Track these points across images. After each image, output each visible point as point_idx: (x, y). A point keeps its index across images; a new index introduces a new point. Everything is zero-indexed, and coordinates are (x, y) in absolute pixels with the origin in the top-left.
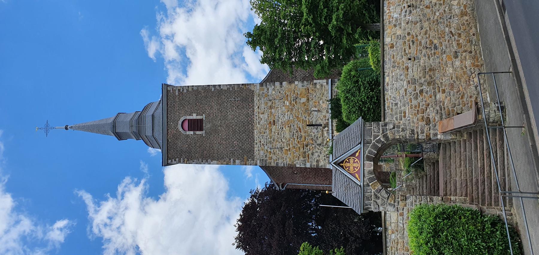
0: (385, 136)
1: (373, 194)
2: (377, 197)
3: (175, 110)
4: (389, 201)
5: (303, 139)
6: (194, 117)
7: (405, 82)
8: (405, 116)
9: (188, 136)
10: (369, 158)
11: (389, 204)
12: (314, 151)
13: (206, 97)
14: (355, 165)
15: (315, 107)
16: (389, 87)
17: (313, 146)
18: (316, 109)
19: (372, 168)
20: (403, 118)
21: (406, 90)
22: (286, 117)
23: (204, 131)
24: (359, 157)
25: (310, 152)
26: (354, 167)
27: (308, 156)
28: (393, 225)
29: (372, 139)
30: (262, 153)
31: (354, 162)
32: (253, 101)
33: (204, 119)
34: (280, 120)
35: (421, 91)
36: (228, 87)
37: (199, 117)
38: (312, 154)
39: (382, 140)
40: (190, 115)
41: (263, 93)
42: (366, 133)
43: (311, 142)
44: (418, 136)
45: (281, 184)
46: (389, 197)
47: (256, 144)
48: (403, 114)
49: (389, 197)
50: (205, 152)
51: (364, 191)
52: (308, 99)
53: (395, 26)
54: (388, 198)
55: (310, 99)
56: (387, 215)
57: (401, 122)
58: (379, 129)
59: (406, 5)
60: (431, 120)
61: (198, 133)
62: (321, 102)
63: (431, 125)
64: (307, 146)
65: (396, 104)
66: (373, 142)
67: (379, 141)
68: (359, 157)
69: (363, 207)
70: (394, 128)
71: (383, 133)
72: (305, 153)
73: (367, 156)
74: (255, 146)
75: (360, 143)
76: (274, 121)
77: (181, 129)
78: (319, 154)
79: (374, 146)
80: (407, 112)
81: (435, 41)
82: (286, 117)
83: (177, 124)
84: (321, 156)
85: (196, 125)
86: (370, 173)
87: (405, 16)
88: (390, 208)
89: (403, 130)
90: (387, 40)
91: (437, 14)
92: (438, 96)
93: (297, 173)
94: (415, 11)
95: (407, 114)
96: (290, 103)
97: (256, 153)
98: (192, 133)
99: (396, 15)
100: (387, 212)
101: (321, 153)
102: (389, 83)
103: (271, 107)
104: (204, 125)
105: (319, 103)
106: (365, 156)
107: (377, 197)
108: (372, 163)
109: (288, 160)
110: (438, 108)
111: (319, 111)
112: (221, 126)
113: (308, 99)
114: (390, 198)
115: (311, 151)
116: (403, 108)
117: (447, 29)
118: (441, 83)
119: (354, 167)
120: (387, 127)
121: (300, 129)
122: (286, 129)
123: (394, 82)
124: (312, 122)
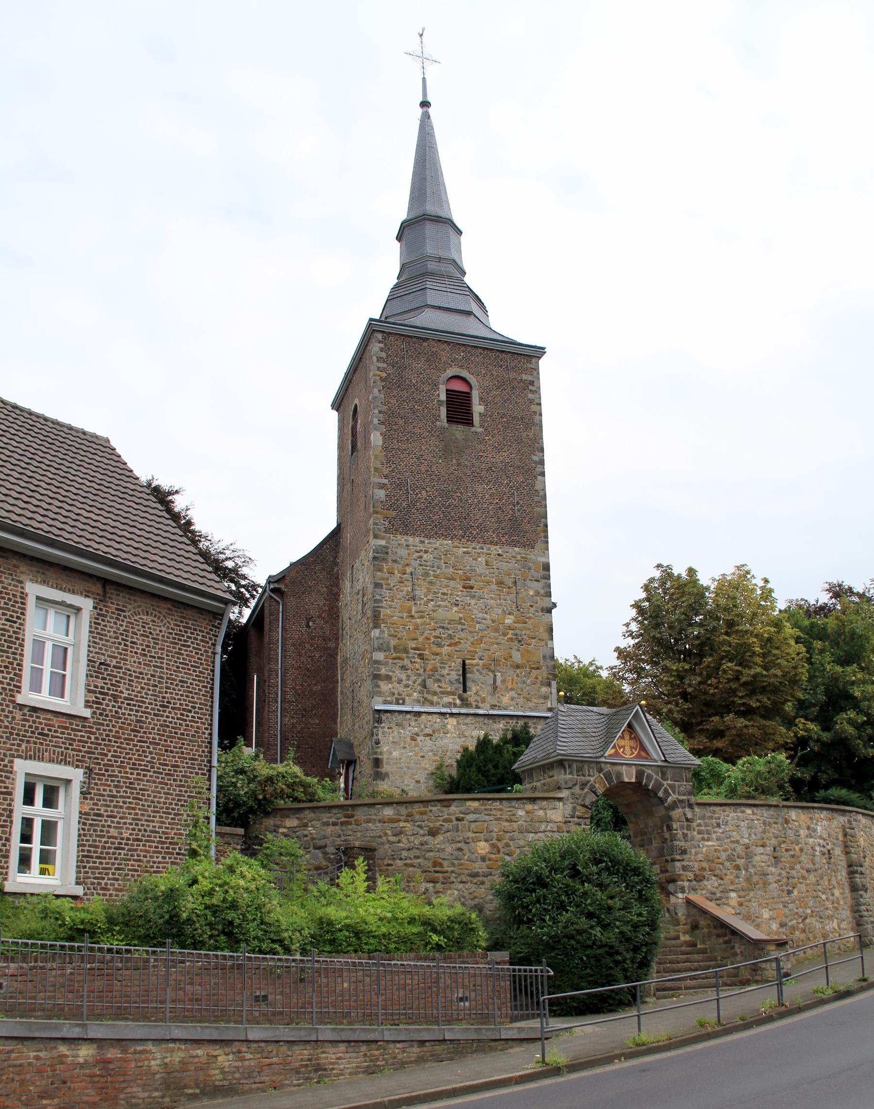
0: (674, 805)
1: (587, 778)
2: (583, 785)
3: (490, 367)
4: (579, 808)
5: (435, 649)
6: (477, 408)
7: (747, 841)
8: (703, 839)
9: (435, 386)
10: (640, 774)
11: (574, 808)
12: (409, 672)
13: (519, 441)
14: (627, 748)
15: (503, 681)
16: (739, 814)
17: (421, 671)
18: (498, 683)
19: (626, 780)
20: (700, 836)
21: (737, 842)
22: (480, 615)
23: (446, 425)
24: (639, 756)
25: (406, 662)
26: (624, 747)
27: (400, 658)
28: (541, 813)
29: (669, 782)
30: (403, 552)
31: (631, 748)
32: (513, 543)
33: (473, 429)
34: (473, 602)
35: (737, 868)
36: (541, 493)
37: (476, 419)
38: (403, 668)
39: (670, 799)
40: (481, 398)
41: (529, 569)
42: (677, 770)
43: (429, 667)
44: (679, 860)
45: (282, 587)
46: (586, 807)
47: (422, 542)
48: (706, 836)
49: (586, 807)
50: (402, 422)
51: (591, 762)
52: (518, 667)
53: (808, 828)
54: (584, 806)
55: (518, 671)
56: (557, 803)
57: (695, 833)
58: (684, 795)
59: (829, 847)
60: (701, 883)
61: (443, 411)
62: (512, 694)
63: (694, 882)
64: (421, 656)
65: (718, 825)
66: (665, 783)
67: (667, 794)
68: (639, 756)
69: (566, 760)
70: (687, 820)
71: (680, 801)
72: (406, 651)
73: (643, 772)
74: (417, 539)
75: (666, 761)
76: (472, 588)
77: (450, 373)
78: (404, 682)
79: (658, 785)
80: (710, 843)
81: (796, 892)
82: (480, 615)
83: (461, 367)
84: (400, 688)
85: (459, 408)
86: (619, 775)
87: (819, 845)
88: (569, 807)
89: (685, 836)
90: (793, 814)
91: (824, 897)
92: (733, 895)
93: (308, 626)
94: (824, 861)
95: (706, 843)
96: (510, 628)
97: (402, 539)
98: (443, 397)
99: (819, 829)
100: (561, 804)
101: (407, 686)
102: (745, 815)
103: (500, 583)
104: (461, 427)
105: (512, 689)
106: (643, 768)
107: (583, 785)
108: (633, 780)
109: (388, 611)
110: (718, 895)
111: (495, 688)
112: (459, 465)
113: (518, 667)
114: (583, 810)
115: (410, 665)
116: (714, 836)
117: (809, 911)
118: (750, 901)
119: (624, 747)
120: (687, 809)
121: (456, 644)
122: (454, 613)
123: (746, 822)
124: (472, 672)
